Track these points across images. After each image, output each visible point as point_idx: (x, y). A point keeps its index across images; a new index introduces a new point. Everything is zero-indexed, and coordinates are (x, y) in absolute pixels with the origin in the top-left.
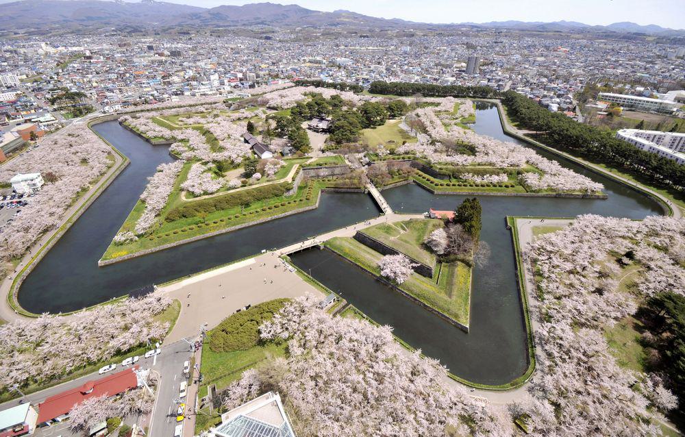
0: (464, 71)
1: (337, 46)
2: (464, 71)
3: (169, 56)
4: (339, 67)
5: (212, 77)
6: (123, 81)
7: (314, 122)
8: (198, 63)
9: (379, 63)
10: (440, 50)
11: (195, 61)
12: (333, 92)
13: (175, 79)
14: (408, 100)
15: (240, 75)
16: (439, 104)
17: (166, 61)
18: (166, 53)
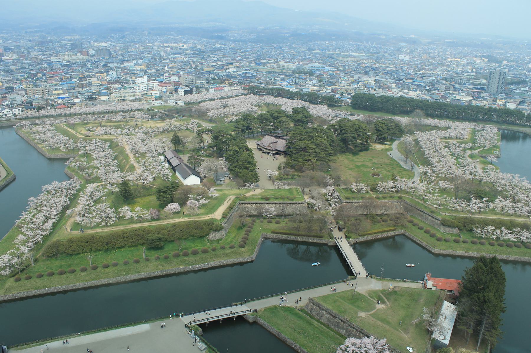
0: (484, 89)
1: (310, 50)
2: (484, 89)
3: (93, 56)
4: (311, 73)
5: (139, 80)
6: (33, 82)
7: (267, 140)
8: (126, 64)
9: (366, 73)
10: (451, 62)
11: (123, 61)
12: (298, 104)
13: (94, 81)
14: (403, 120)
15: (175, 79)
16: (448, 128)
17: (88, 61)
18: (91, 52)
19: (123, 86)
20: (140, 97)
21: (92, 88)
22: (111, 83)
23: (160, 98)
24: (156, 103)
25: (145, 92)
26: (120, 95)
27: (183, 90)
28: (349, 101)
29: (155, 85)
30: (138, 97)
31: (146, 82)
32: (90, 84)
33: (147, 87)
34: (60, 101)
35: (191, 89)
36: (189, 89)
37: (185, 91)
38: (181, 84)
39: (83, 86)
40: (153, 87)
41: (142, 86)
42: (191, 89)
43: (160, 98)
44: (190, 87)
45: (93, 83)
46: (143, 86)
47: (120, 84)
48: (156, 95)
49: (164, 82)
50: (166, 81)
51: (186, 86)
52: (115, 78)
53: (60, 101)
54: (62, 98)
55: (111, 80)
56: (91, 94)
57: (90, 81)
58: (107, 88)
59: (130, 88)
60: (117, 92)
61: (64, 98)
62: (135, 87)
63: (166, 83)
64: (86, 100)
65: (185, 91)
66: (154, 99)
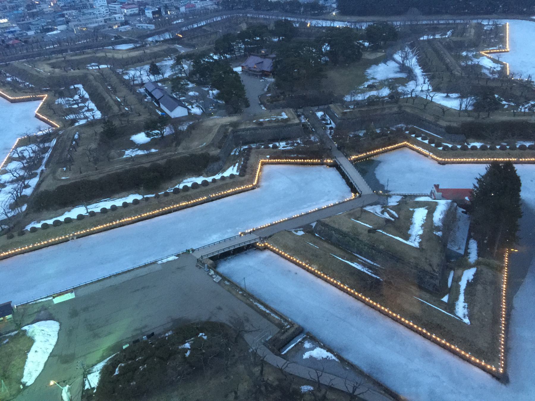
19: (80, 11)
20: (103, 23)
21: (44, 16)
22: (66, 10)
23: (126, 23)
24: (123, 28)
25: (108, 17)
26: (80, 23)
27: (150, 11)
28: (334, 6)
29: (118, 7)
30: (101, 24)
31: (106, 5)
32: (41, 13)
33: (108, 11)
34: (10, 36)
35: (160, 9)
36: (157, 9)
37: (152, 12)
38: (146, 4)
39: (33, 15)
40: (116, 10)
41: (103, 10)
42: (160, 9)
43: (126, 23)
44: (158, 6)
45: (45, 10)
46: (104, 10)
47: (76, 9)
48: (121, 19)
49: (126, 3)
50: (129, 2)
51: (153, 5)
52: (69, 3)
53: (10, 36)
54: (12, 32)
55: (65, 6)
56: (45, 24)
57: (41, 8)
58: (63, 16)
59: (90, 14)
60: (76, 20)
61: (15, 31)
62: (95, 12)
63: (129, 4)
64: (41, 32)
65: (152, 12)
66: (119, 25)
